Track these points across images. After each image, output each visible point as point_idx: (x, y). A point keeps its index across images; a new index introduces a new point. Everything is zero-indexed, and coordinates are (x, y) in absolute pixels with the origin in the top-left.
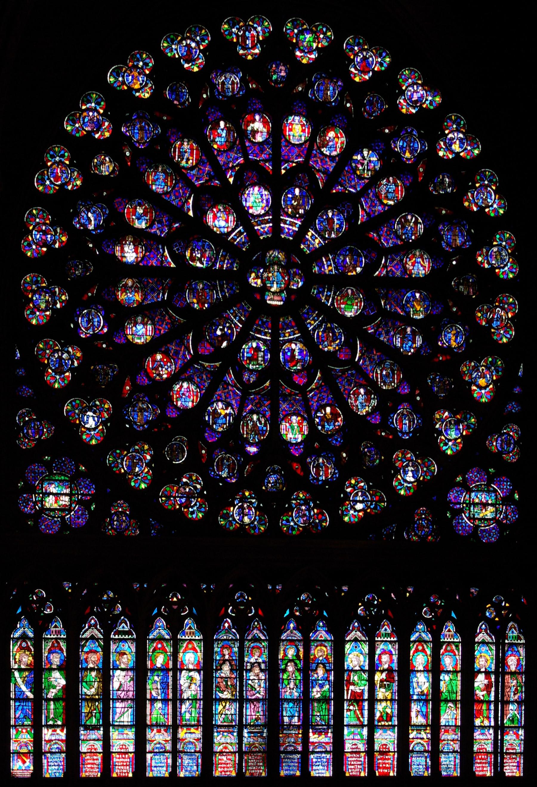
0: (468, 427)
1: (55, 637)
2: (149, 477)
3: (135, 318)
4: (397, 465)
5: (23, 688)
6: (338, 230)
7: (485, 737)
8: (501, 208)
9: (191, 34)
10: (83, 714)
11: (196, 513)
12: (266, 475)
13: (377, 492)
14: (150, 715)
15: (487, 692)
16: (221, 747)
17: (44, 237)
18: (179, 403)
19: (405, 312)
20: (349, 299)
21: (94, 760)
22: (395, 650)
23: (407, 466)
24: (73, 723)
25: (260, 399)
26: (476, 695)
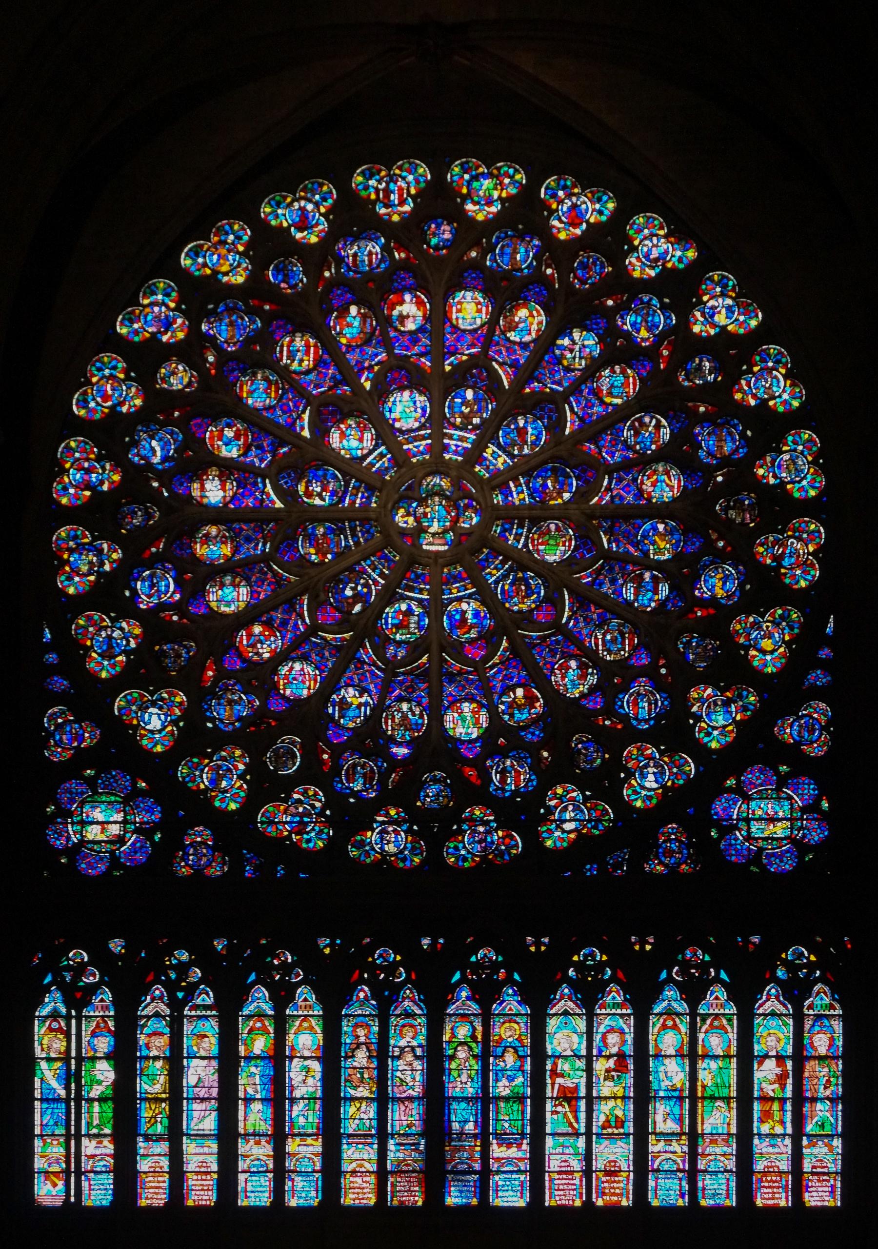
0: (745, 708)
1: (102, 1013)
3: (221, 578)
4: (630, 765)
5: (54, 1084)
7: (776, 1150)
8: (795, 398)
10: (143, 1120)
11: (315, 840)
12: (423, 785)
16: (354, 1165)
17: (86, 477)
18: (288, 692)
19: (641, 550)
20: (551, 537)
22: (629, 1026)
23: (646, 766)
24: (126, 1132)
25: (412, 681)
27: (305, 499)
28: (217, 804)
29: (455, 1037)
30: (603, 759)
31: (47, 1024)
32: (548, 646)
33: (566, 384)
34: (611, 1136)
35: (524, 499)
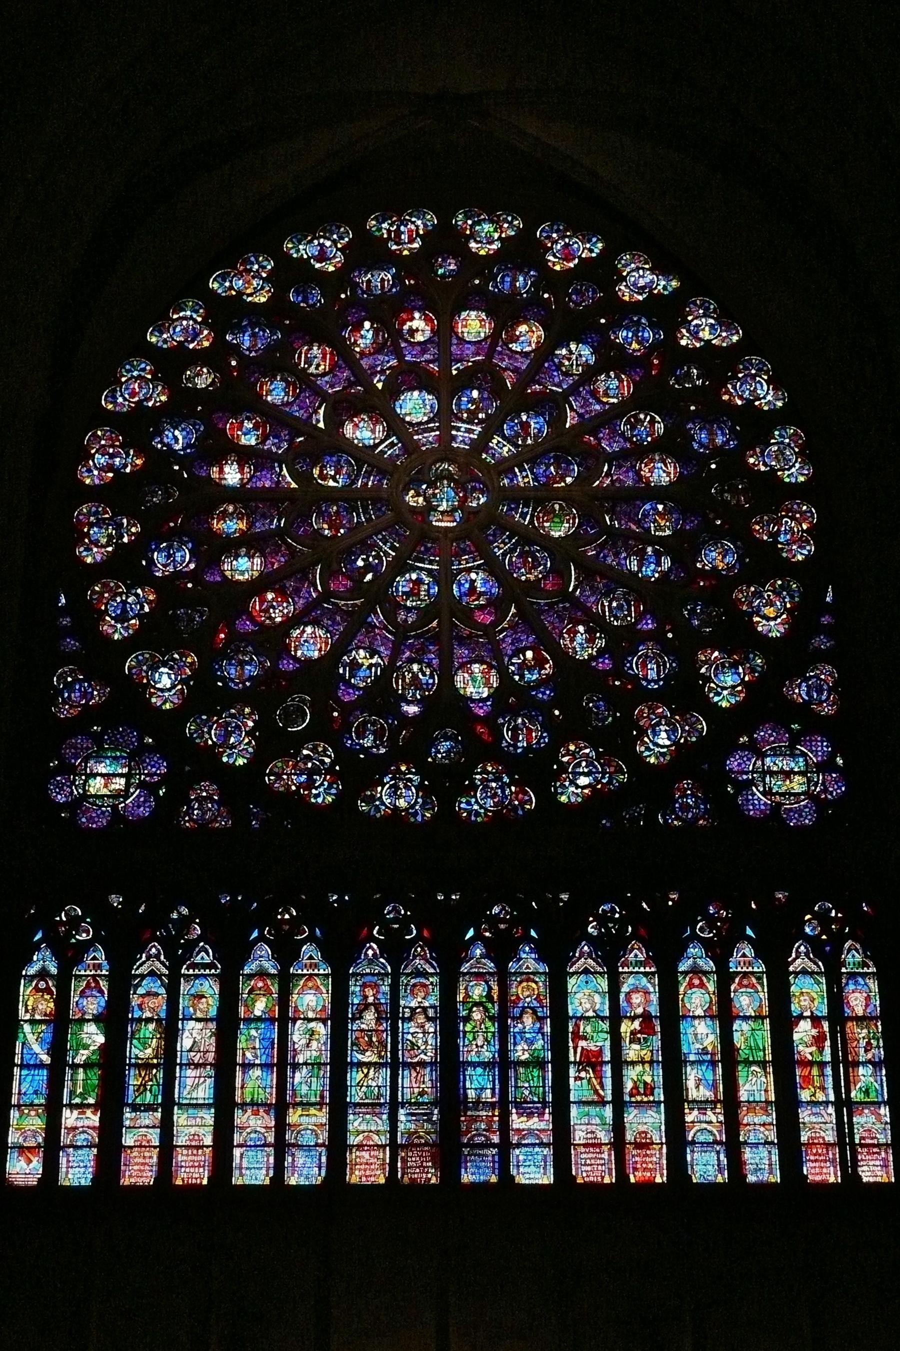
0: (752, 670)
1: (93, 972)
2: (251, 750)
4: (641, 723)
5: (36, 1048)
6: (536, 437)
7: (820, 1120)
8: (779, 400)
9: (325, 233)
10: (131, 1088)
11: (323, 795)
12: (434, 742)
13: (610, 761)
14: (242, 1087)
15: (818, 1047)
18: (299, 653)
21: (144, 1157)
22: (654, 986)
23: (658, 724)
26: (799, 1053)
27: (319, 481)
28: (225, 759)
29: (470, 997)
30: (614, 716)
31: (34, 984)
32: (556, 612)
33: (565, 387)
34: (639, 1104)
35: (529, 482)
